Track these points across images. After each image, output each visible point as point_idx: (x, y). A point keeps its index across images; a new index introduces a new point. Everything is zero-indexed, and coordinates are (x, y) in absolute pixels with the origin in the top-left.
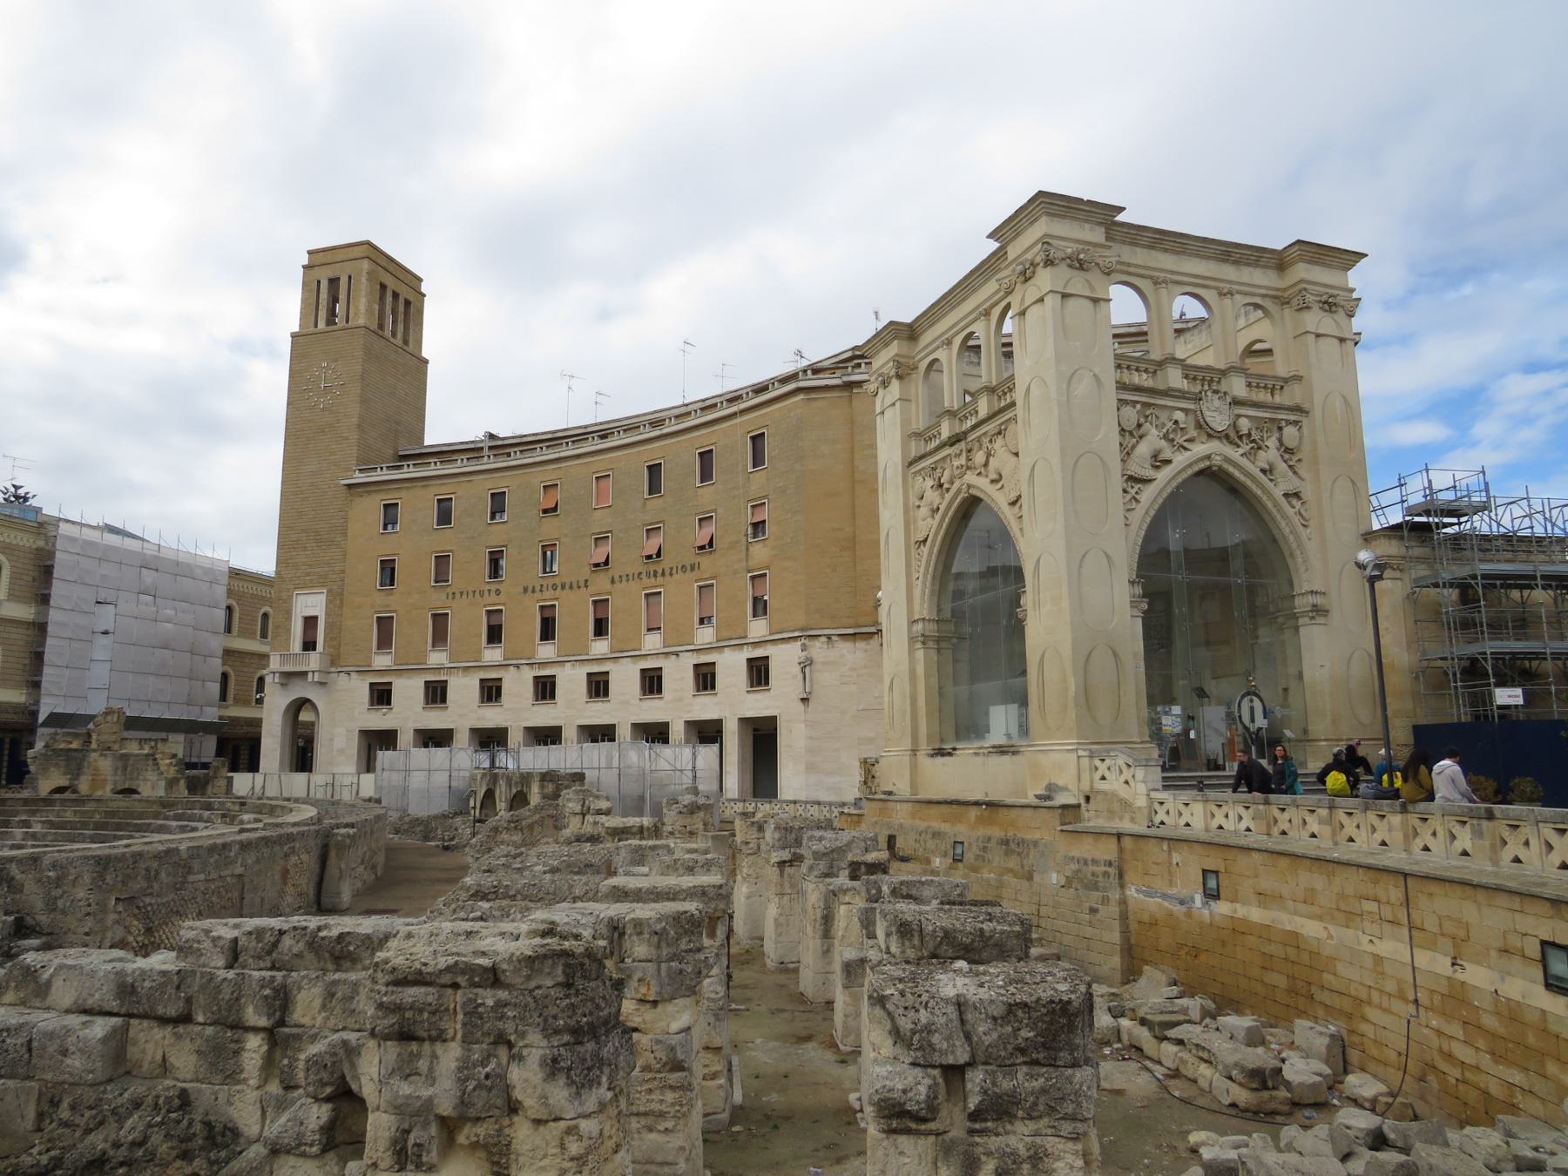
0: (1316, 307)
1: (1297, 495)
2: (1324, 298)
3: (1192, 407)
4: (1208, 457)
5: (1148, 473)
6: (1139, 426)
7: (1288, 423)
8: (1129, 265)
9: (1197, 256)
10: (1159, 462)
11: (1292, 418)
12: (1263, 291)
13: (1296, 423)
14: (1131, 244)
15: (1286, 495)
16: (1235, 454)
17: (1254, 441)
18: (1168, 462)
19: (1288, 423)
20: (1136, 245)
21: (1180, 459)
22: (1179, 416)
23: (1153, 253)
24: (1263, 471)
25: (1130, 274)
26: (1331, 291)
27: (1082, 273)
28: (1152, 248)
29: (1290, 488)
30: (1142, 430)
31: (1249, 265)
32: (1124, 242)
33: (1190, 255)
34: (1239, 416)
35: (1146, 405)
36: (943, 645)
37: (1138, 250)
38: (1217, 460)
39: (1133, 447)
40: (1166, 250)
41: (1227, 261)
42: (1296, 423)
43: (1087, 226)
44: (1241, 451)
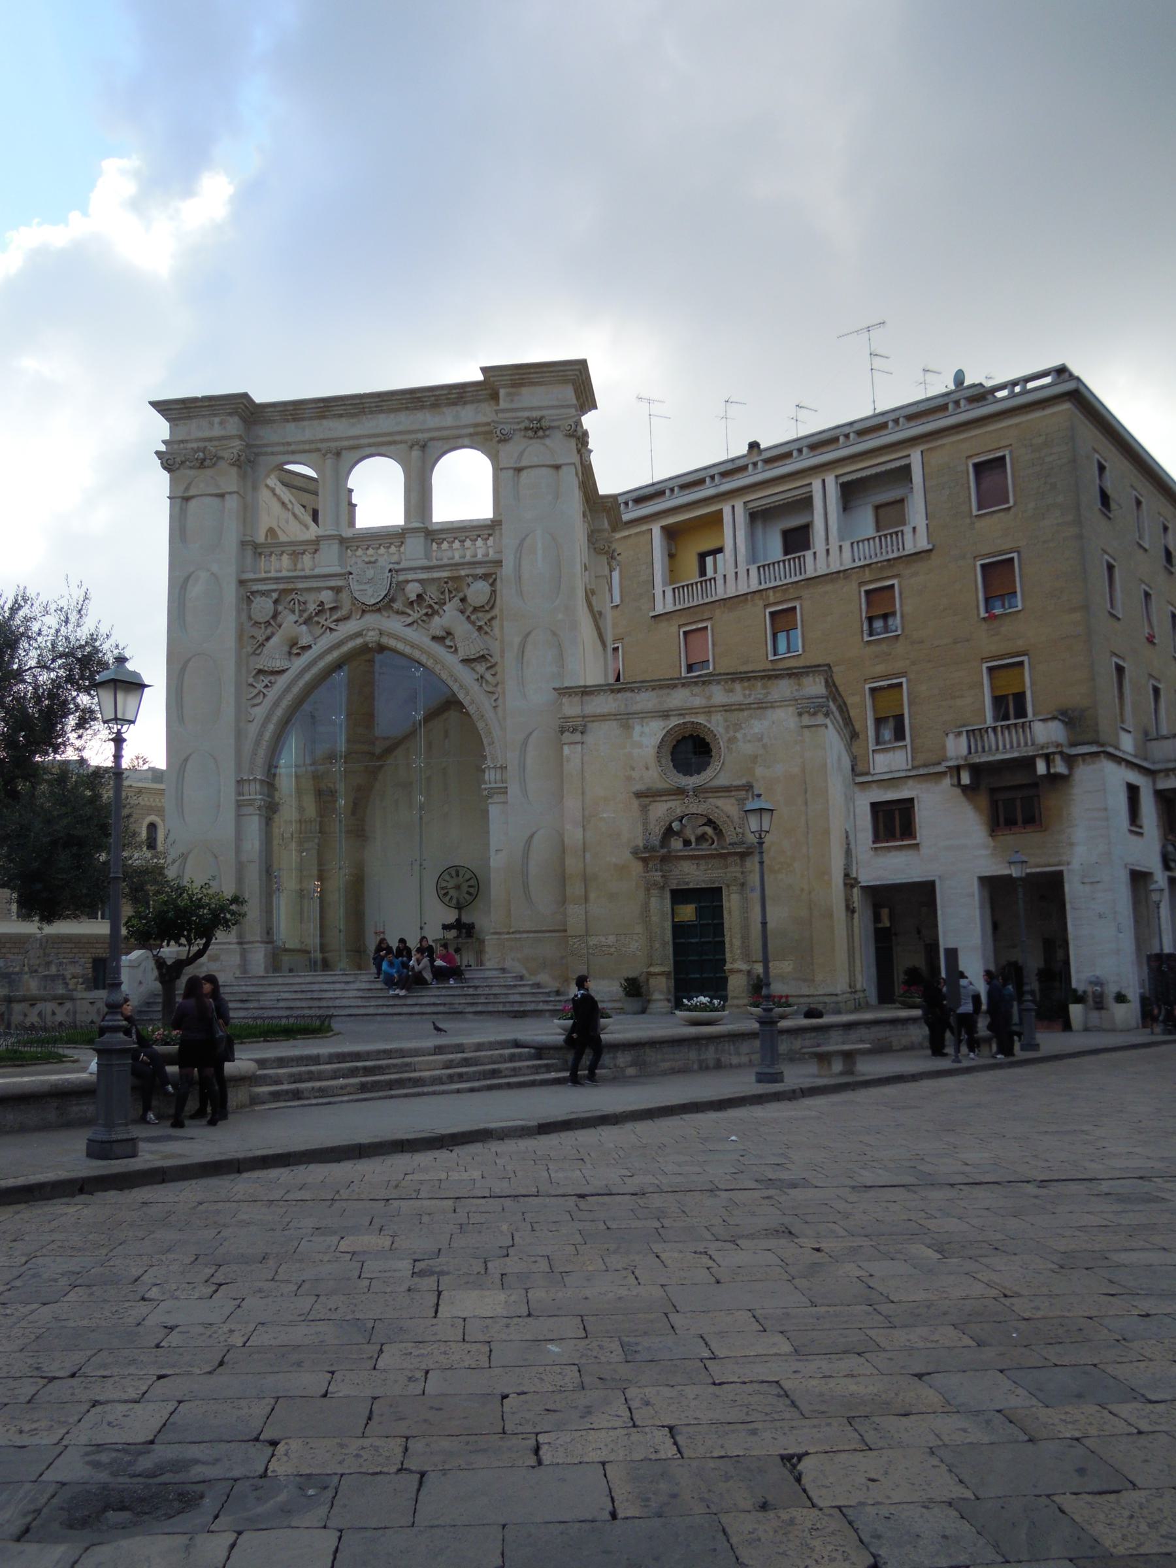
0: (518, 437)
1: (483, 658)
2: (526, 424)
3: (340, 583)
4: (359, 634)
5: (284, 664)
6: (275, 616)
7: (476, 577)
8: (289, 444)
9: (382, 411)
10: (295, 648)
11: (480, 571)
12: (471, 430)
13: (485, 577)
14: (294, 420)
15: (466, 661)
16: (393, 624)
17: (430, 606)
18: (310, 647)
19: (476, 577)
20: (303, 419)
21: (327, 640)
22: (327, 597)
23: (325, 422)
24: (434, 638)
25: (293, 452)
26: (535, 414)
27: (209, 472)
28: (324, 417)
29: (473, 651)
30: (279, 619)
31: (455, 404)
32: (288, 421)
33: (371, 412)
34: (407, 582)
35: (284, 590)
36: (306, 845)
37: (306, 423)
38: (371, 637)
39: (268, 639)
40: (341, 416)
41: (423, 407)
42: (485, 577)
43: (217, 420)
44: (410, 620)
